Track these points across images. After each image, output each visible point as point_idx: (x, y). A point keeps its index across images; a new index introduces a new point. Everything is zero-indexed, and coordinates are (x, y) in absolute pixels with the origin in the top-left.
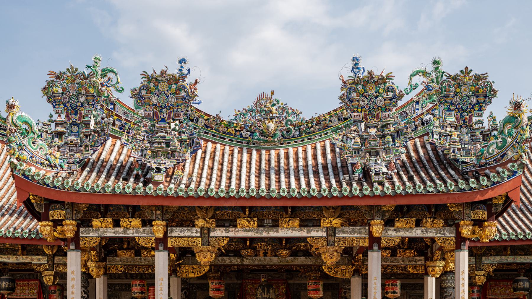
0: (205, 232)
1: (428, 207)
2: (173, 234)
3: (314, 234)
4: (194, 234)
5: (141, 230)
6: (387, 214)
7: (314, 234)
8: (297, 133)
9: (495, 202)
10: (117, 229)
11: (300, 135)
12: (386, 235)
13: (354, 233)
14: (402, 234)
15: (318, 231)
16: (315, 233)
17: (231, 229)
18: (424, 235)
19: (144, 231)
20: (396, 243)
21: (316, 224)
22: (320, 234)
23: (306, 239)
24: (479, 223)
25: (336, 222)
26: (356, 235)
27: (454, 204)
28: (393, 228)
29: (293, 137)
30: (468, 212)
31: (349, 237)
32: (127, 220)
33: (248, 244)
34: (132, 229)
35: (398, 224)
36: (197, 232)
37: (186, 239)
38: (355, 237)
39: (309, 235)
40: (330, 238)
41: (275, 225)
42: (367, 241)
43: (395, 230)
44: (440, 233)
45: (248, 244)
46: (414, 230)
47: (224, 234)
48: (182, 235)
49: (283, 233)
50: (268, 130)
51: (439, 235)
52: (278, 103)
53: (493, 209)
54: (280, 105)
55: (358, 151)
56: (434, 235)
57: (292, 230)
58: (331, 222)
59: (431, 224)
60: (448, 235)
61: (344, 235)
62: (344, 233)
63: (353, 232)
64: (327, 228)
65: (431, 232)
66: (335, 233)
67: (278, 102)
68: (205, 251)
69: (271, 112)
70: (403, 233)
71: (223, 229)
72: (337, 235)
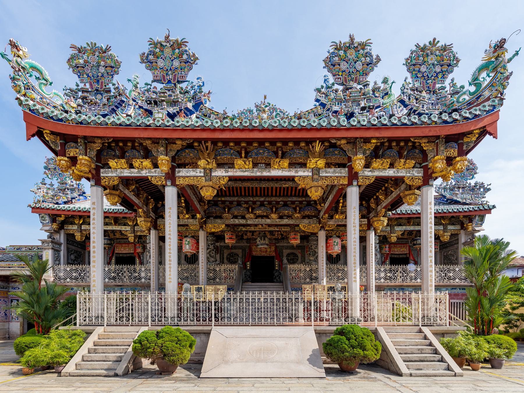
0: (208, 173)
2: (181, 174)
4: (198, 174)
5: (153, 170)
6: (368, 152)
10: (132, 170)
12: (363, 174)
15: (304, 172)
16: (302, 173)
17: (230, 170)
19: (155, 171)
20: (372, 182)
21: (303, 165)
22: (306, 174)
25: (321, 163)
26: (337, 175)
28: (369, 170)
32: (138, 160)
34: (143, 169)
36: (200, 172)
37: (192, 178)
39: (297, 175)
40: (316, 177)
41: (268, 165)
43: (370, 171)
46: (387, 171)
47: (224, 174)
48: (188, 175)
49: (275, 173)
52: (270, 105)
54: (271, 106)
57: (283, 171)
61: (327, 175)
62: (326, 172)
63: (334, 172)
66: (319, 174)
67: (270, 104)
68: (208, 186)
71: (223, 170)
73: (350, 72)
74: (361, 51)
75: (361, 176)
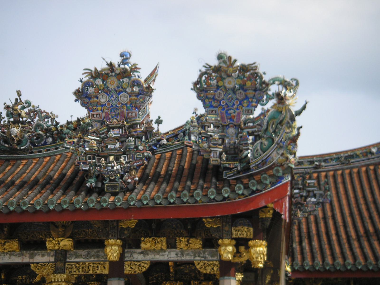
1: (184, 222)
3: (38, 259)
6: (126, 232)
7: (38, 259)
8: (50, 140)
9: (262, 215)
11: (54, 141)
12: (131, 258)
13: (91, 257)
14: (151, 257)
15: (43, 256)
18: (179, 259)
21: (40, 245)
22: (46, 259)
23: (30, 266)
24: (241, 243)
25: (66, 243)
26: (92, 259)
27: (211, 218)
28: (140, 251)
29: (45, 143)
30: (227, 228)
31: (84, 263)
33: (3, 277)
35: (143, 246)
38: (91, 261)
39: (31, 261)
40: (60, 264)
42: (107, 266)
43: (142, 253)
44: (199, 256)
45: (3, 277)
46: (167, 253)
50: (11, 135)
51: (197, 258)
53: (260, 224)
55: (95, 154)
56: (192, 258)
57: (11, 255)
58: (59, 244)
59: (187, 245)
60: (210, 258)
62: (77, 257)
63: (89, 255)
64: (56, 251)
65: (188, 255)
66: (65, 258)
69: (20, 115)
70: (153, 255)
72: (68, 260)
73: (112, 106)
74: (126, 80)
75: (127, 261)
